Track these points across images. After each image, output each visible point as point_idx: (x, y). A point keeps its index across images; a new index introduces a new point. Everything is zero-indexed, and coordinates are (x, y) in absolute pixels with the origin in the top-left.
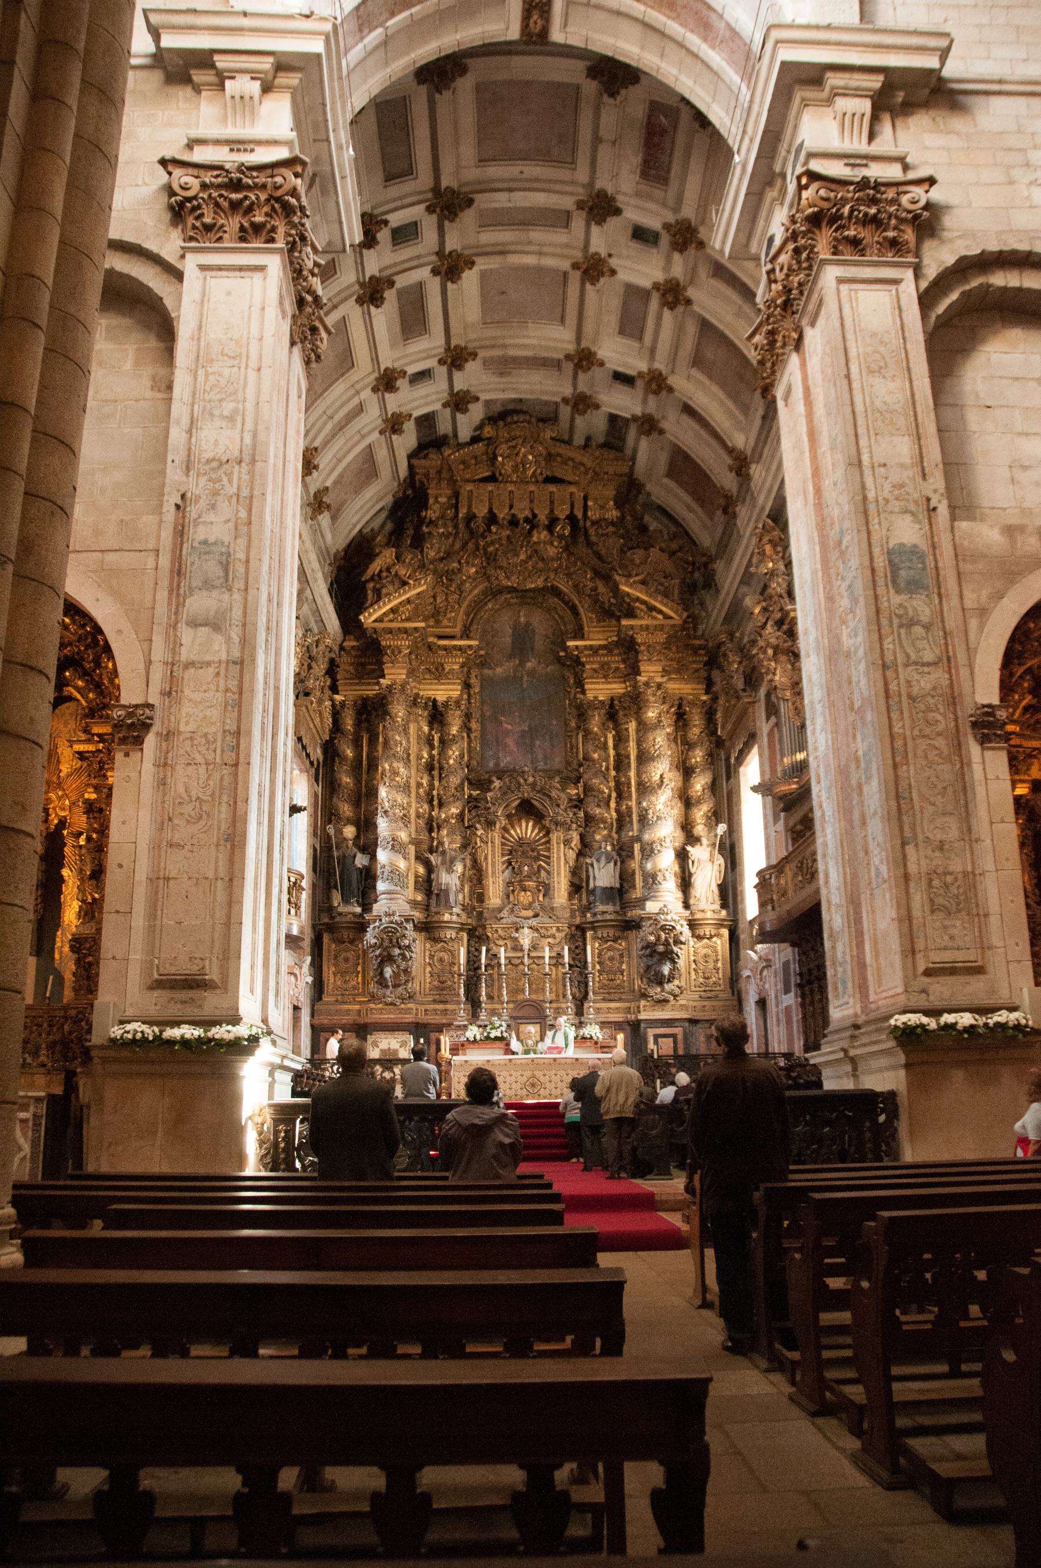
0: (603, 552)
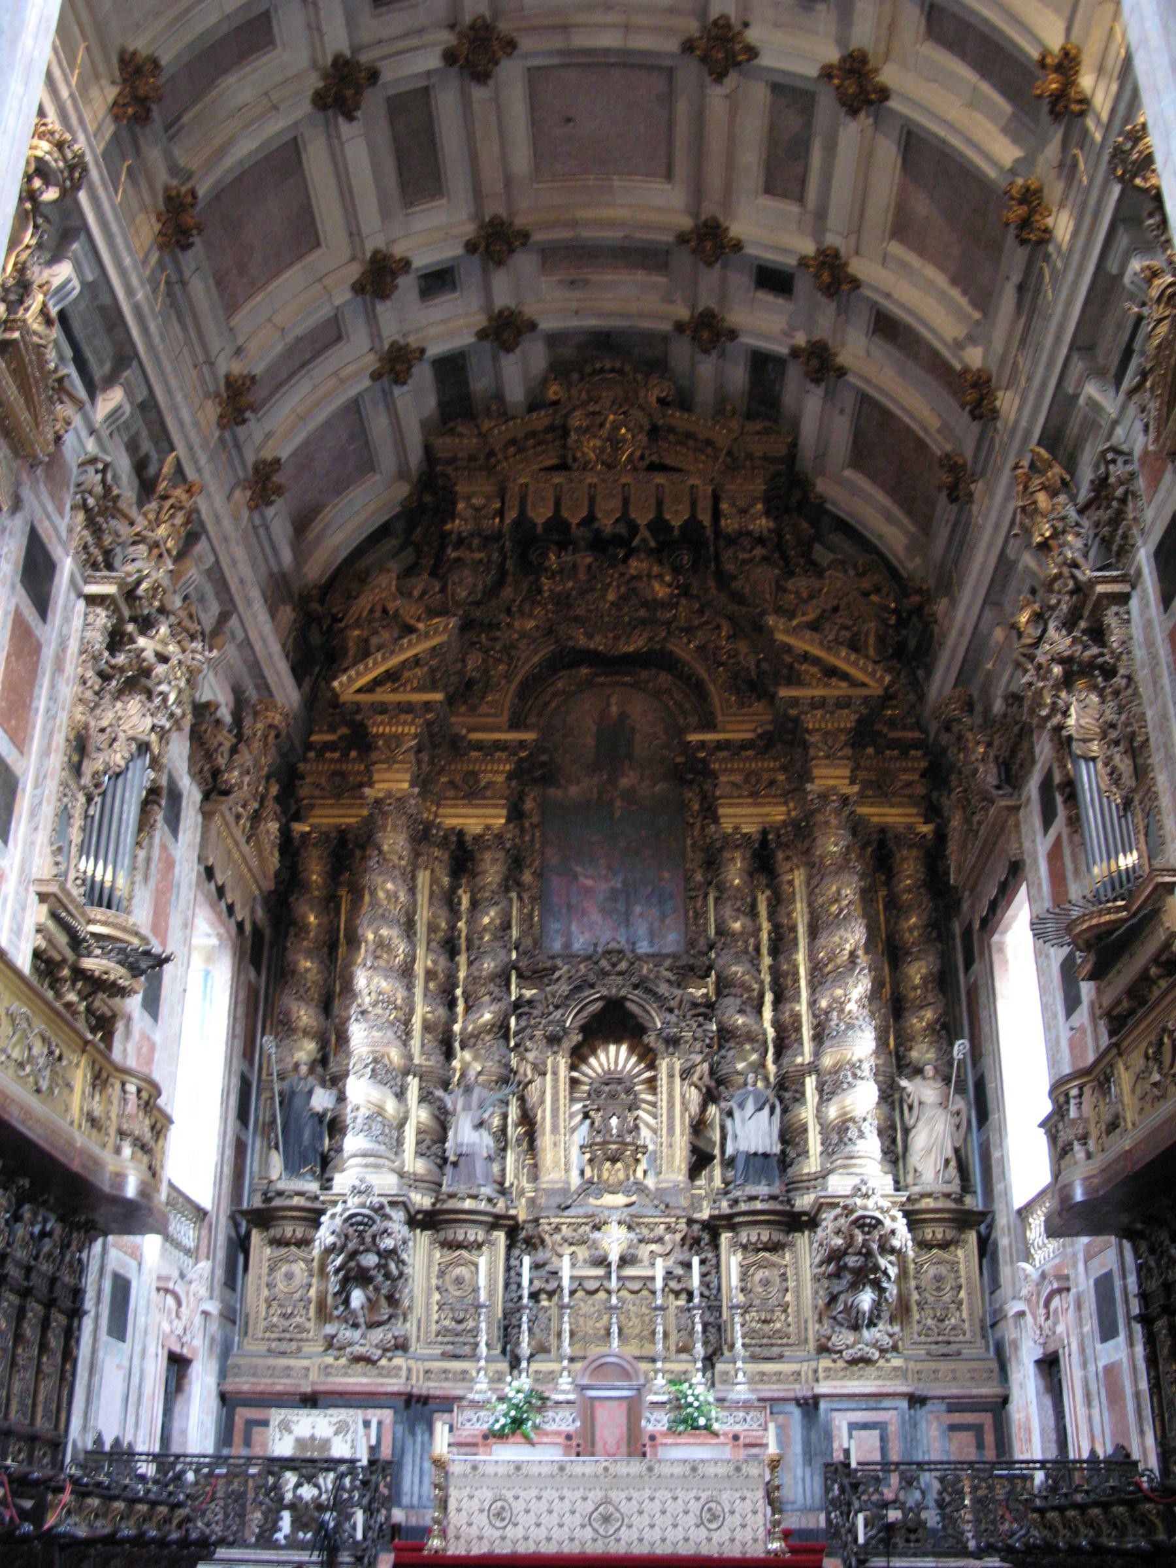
0: (747, 590)
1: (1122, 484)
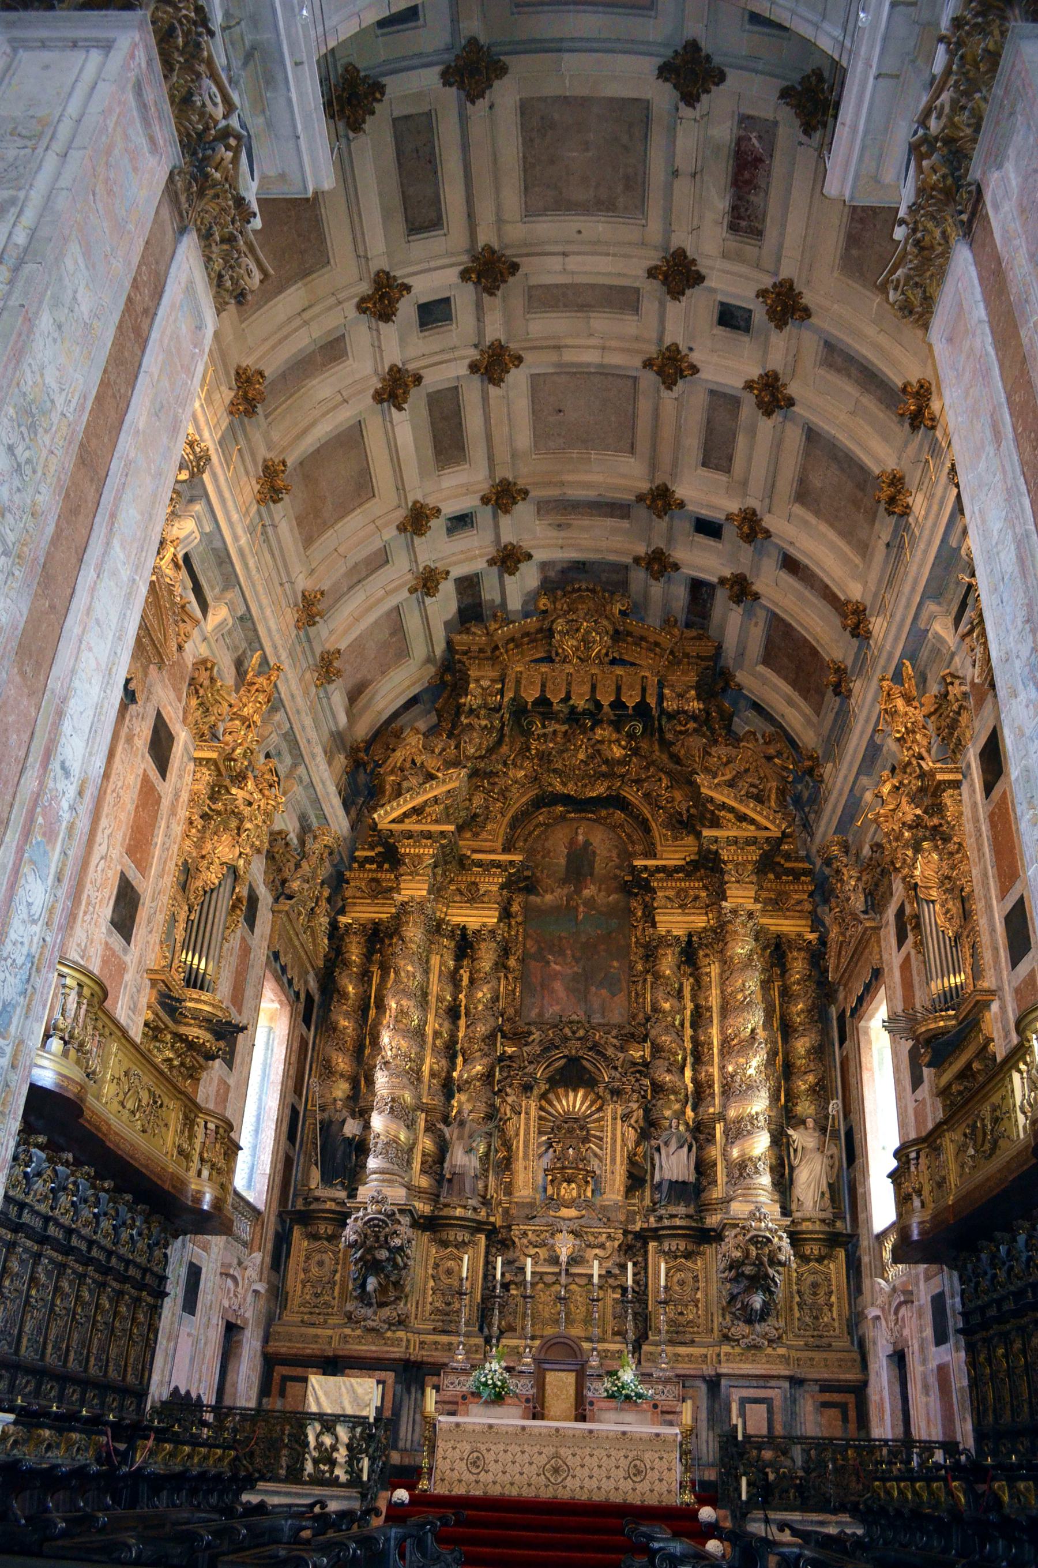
1: (957, 700)
